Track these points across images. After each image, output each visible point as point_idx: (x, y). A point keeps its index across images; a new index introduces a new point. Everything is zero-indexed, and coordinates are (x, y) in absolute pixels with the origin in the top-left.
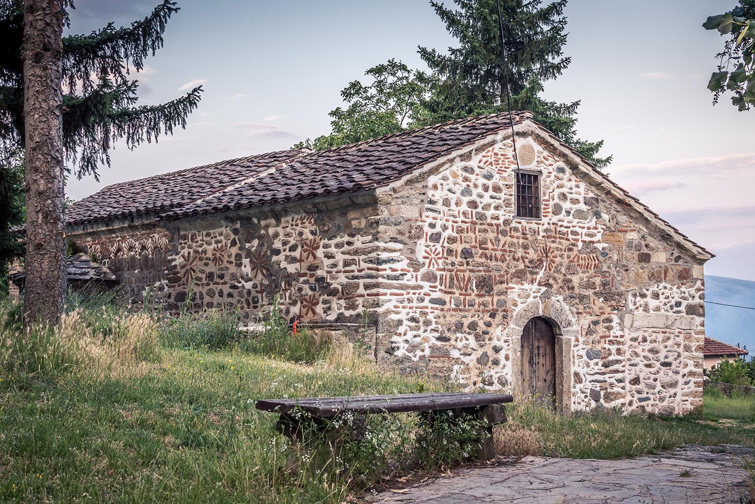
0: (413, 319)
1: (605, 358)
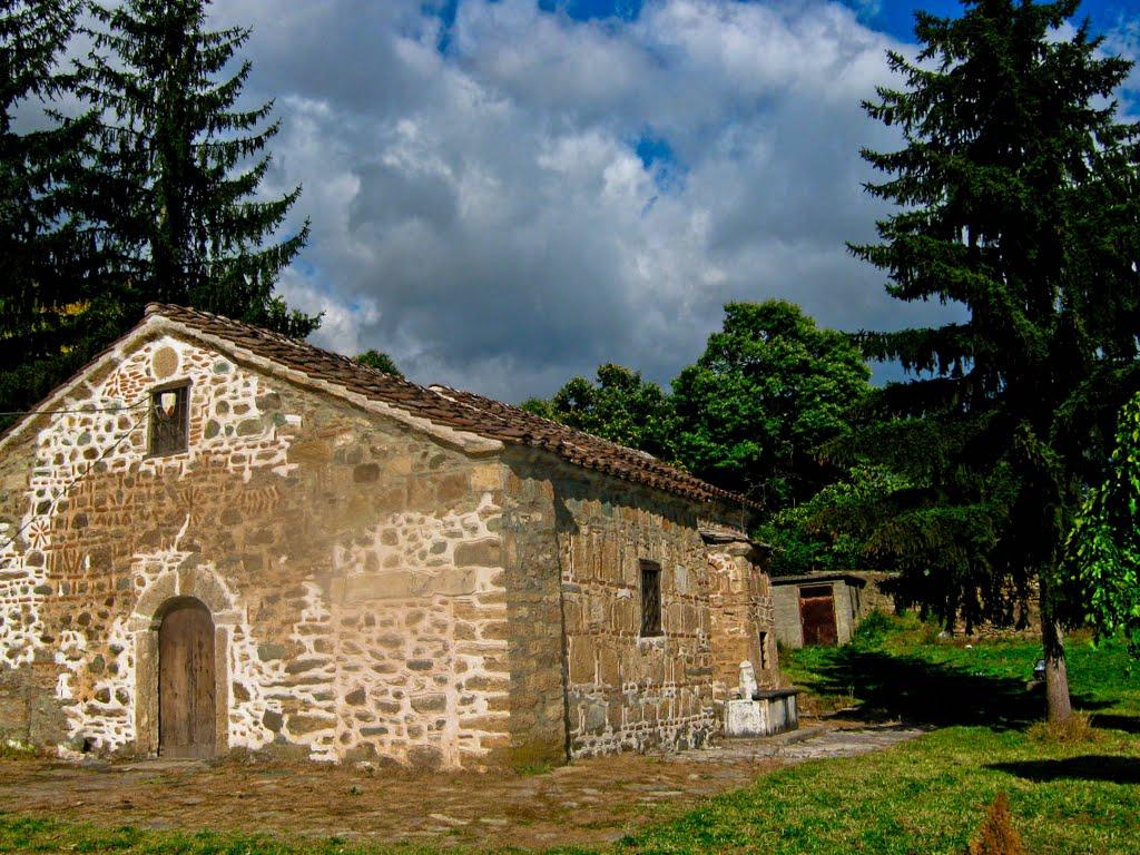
0: (15, 616)
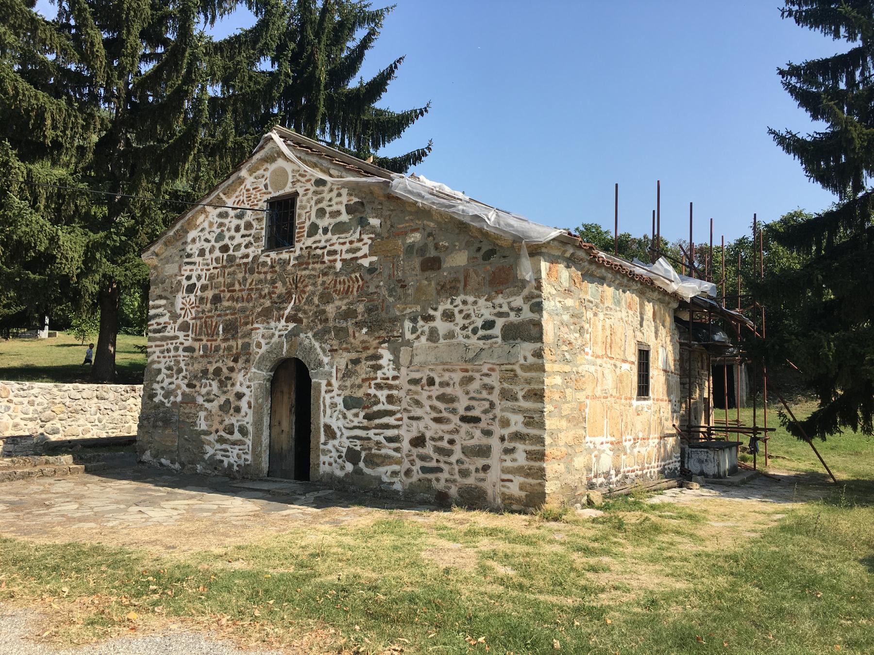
0: (169, 368)
1: (368, 407)
